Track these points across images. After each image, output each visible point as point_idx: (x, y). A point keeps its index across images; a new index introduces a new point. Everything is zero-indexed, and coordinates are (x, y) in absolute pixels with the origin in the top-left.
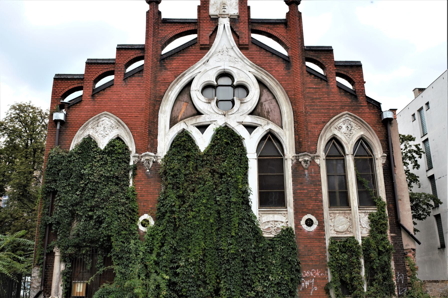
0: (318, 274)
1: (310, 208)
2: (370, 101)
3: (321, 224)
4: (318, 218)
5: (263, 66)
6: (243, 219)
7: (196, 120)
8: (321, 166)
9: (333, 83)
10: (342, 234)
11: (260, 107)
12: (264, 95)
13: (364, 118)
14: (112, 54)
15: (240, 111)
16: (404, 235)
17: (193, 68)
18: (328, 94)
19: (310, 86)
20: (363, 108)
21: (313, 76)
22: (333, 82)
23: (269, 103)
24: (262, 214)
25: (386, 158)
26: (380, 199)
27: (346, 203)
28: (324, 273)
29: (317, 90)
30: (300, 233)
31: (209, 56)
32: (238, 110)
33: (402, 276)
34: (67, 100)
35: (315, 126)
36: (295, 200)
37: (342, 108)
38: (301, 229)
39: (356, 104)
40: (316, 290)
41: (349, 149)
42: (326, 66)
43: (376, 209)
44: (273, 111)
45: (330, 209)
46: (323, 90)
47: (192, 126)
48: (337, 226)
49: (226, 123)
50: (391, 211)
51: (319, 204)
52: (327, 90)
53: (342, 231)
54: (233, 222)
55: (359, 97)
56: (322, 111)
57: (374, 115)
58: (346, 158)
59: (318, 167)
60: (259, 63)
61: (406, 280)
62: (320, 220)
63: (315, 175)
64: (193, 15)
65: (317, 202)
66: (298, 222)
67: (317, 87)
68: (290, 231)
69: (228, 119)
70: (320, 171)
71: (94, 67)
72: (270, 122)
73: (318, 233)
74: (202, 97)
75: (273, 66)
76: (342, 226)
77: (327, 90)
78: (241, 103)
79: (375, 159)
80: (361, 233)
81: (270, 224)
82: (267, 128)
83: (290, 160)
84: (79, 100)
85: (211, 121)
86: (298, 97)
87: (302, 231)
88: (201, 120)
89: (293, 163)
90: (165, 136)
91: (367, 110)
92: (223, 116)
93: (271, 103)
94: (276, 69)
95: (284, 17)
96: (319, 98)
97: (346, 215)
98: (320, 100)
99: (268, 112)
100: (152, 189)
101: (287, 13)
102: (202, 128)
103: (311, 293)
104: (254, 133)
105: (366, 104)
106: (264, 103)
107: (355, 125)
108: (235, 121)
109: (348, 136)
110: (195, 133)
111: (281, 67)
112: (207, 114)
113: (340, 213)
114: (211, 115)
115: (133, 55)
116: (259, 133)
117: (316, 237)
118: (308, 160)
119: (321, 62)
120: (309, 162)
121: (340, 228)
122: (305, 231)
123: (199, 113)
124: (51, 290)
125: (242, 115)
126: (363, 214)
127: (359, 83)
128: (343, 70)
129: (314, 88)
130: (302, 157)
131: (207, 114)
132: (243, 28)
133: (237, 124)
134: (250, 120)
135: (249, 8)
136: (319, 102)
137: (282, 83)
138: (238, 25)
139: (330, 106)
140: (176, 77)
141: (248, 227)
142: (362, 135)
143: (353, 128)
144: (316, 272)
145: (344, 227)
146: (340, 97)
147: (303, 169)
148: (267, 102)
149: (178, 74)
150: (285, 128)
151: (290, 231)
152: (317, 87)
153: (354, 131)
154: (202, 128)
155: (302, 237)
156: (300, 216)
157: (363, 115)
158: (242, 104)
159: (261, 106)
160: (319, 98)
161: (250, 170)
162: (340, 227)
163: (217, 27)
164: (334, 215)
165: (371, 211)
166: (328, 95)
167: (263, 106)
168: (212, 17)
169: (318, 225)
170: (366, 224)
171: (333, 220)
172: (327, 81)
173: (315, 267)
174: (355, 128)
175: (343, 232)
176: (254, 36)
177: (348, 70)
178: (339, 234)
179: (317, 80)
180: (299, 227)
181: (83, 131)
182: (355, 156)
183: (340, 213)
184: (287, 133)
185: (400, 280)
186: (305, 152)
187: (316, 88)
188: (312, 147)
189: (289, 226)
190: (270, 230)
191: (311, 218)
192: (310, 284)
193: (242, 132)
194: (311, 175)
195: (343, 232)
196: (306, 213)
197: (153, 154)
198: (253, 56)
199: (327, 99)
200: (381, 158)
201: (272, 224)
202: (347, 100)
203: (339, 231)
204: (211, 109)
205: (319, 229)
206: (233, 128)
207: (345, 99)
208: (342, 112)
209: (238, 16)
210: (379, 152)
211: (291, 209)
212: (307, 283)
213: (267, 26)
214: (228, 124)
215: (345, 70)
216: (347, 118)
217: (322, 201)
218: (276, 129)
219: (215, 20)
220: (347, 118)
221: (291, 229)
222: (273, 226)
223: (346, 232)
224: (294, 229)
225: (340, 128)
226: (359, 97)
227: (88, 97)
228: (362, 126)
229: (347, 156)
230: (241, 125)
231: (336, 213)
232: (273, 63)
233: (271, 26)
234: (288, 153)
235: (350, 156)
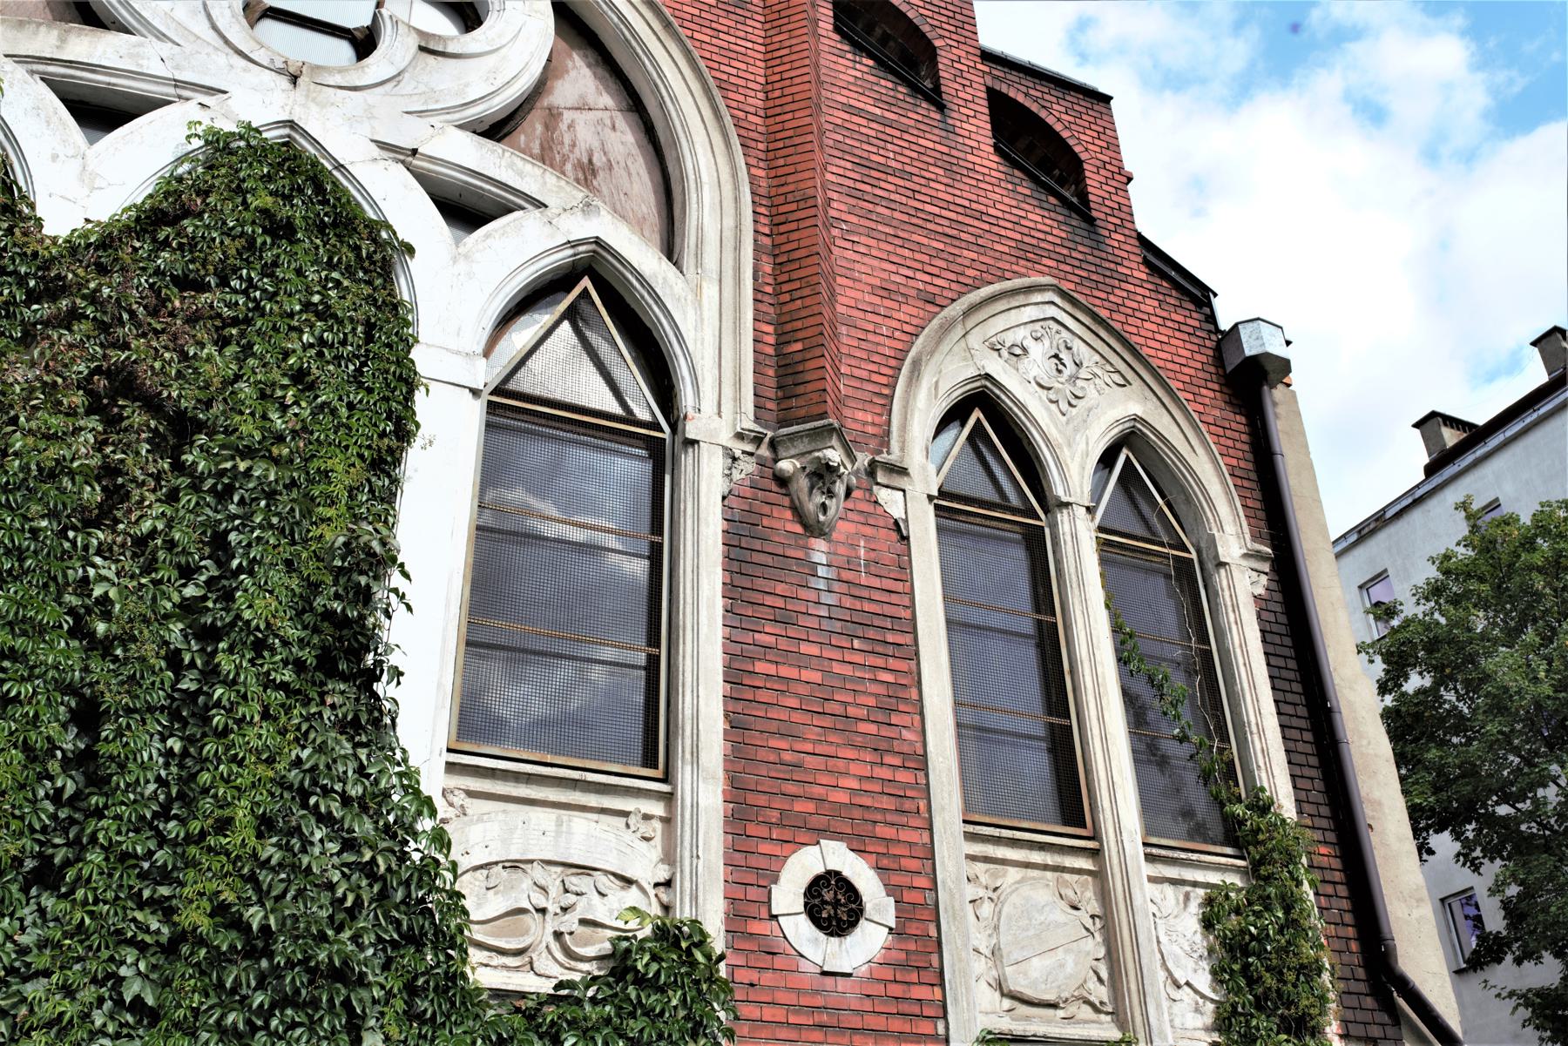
1: (842, 797)
2: (1158, 263)
3: (913, 928)
4: (896, 879)
6: (304, 794)
7: (63, 40)
8: (914, 533)
10: (1049, 1021)
11: (539, 128)
12: (573, 74)
15: (407, 85)
19: (852, 102)
21: (871, 63)
23: (600, 122)
24: (471, 794)
25: (1266, 567)
26: (1263, 807)
30: (767, 978)
35: (877, 300)
36: (736, 725)
37: (1028, 254)
38: (772, 952)
42: (937, 43)
43: (1237, 869)
44: (619, 171)
45: (970, 828)
47: (20, 71)
48: (1017, 956)
50: (1329, 889)
51: (903, 776)
53: (1050, 997)
54: (207, 804)
58: (1054, 526)
59: (900, 532)
62: (909, 896)
63: (876, 582)
65: (888, 759)
66: (753, 893)
68: (688, 950)
69: (314, 108)
70: (904, 568)
76: (1048, 961)
79: (1210, 566)
81: (526, 884)
83: (720, 451)
85: (178, 84)
86: (788, 125)
87: (779, 962)
89: (736, 476)
91: (1150, 305)
92: (284, 82)
93: (614, 128)
97: (1067, 884)
104: (487, 236)
105: (1144, 276)
106: (568, 116)
107: (1097, 358)
108: (366, 131)
109: (1064, 406)
112: (162, 36)
113: (1027, 865)
114: (188, 47)
117: (878, 1023)
119: (909, 14)
121: (1032, 977)
122: (804, 966)
125: (420, 113)
126: (1168, 889)
129: (873, 119)
130: (802, 446)
131: (162, 36)
133: (376, 151)
141: (348, 869)
142: (1136, 419)
143: (1083, 373)
145: (1062, 966)
146: (1014, 203)
147: (799, 529)
150: (699, 263)
151: (689, 952)
153: (1091, 392)
155: (779, 1014)
156: (765, 848)
158: (431, 59)
161: (415, 460)
162: (1038, 967)
164: (995, 876)
165: (1214, 878)
167: (563, 126)
170: (1191, 964)
171: (986, 909)
172: (941, 107)
174: (1095, 375)
175: (1054, 1006)
178: (1027, 1018)
179: (890, 85)
180: (755, 927)
182: (1101, 529)
183: (1027, 865)
184: (710, 291)
186: (823, 415)
188: (860, 415)
189: (683, 912)
190: (526, 932)
191: (846, 873)
194: (846, 575)
195: (1054, 1006)
196: (819, 833)
199: (942, 187)
200: (1245, 563)
201: (544, 889)
203: (1030, 993)
204: (202, 16)
206: (340, 167)
207: (1039, 219)
210: (1230, 528)
214: (306, 134)
216: (1052, 311)
217: (920, 762)
220: (1052, 311)
221: (702, 941)
222: (553, 908)
223: (1072, 1009)
224: (718, 945)
225: (1018, 351)
228: (1130, 375)
229: (1063, 518)
230: (400, 166)
231: (1004, 862)
234: (709, 405)
235: (1081, 512)
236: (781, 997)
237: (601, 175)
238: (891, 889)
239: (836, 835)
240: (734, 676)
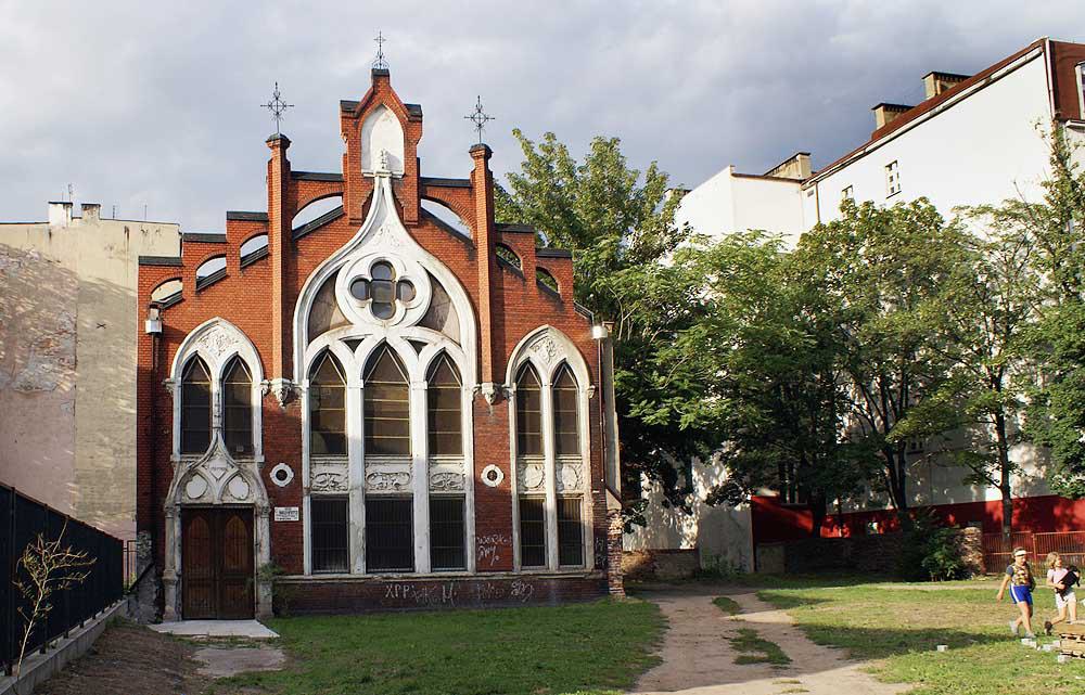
14: (221, 227)
16: (607, 491)
18: (524, 297)
34: (157, 296)
41: (546, 378)
64: (338, 169)
71: (196, 246)
74: (353, 300)
84: (177, 301)
88: (353, 333)
102: (353, 344)
110: (341, 351)
116: (429, 353)
123: (347, 323)
124: (164, 561)
132: (410, 193)
135: (418, 159)
139: (525, 316)
154: (353, 344)
173: (498, 532)
176: (425, 204)
192: (491, 552)
193: (406, 352)
202: (549, 307)
212: (487, 552)
213: (442, 189)
218: (452, 350)
227: (190, 295)
233: (449, 191)
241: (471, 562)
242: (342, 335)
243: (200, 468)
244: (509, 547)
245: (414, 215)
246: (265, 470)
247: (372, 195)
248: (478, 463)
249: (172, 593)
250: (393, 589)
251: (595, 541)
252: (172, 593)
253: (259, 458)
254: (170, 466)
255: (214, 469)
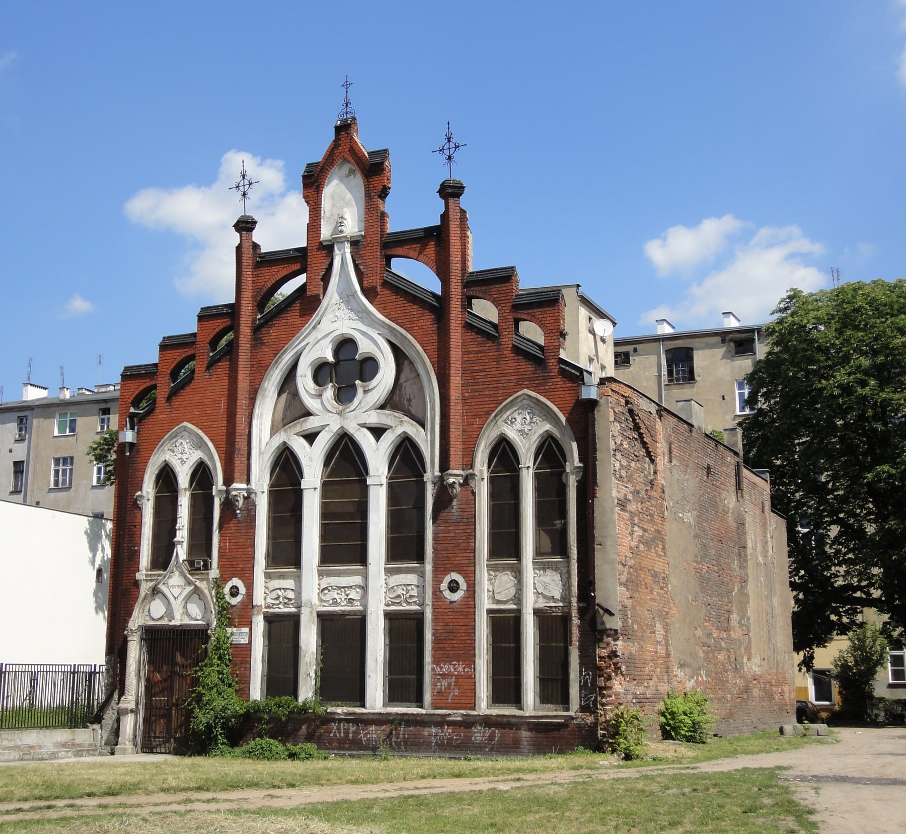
0: (461, 669)
5: (400, 321)
9: (507, 339)
13: (554, 400)
15: (363, 404)
17: (298, 338)
20: (554, 380)
22: (507, 336)
27: (515, 551)
28: (470, 668)
29: (480, 355)
31: (320, 314)
32: (360, 403)
33: (589, 675)
39: (541, 374)
40: (456, 694)
46: (490, 354)
49: (342, 427)
52: (497, 353)
55: (548, 361)
56: (485, 393)
57: (571, 392)
60: (395, 316)
61: (594, 681)
66: (438, 586)
67: (481, 349)
72: (406, 418)
73: (466, 603)
75: (415, 319)
77: (497, 353)
78: (364, 391)
80: (536, 602)
82: (399, 430)
90: (260, 456)
94: (419, 325)
95: (438, 222)
96: (483, 370)
98: (485, 373)
99: (409, 400)
100: (242, 540)
101: (441, 215)
102: (311, 437)
103: (450, 698)
110: (299, 446)
111: (427, 321)
115: (219, 324)
116: (389, 440)
118: (454, 483)
120: (457, 486)
123: (308, 414)
127: (551, 335)
128: (526, 312)
131: (318, 415)
134: (374, 418)
136: (485, 376)
137: (428, 348)
138: (362, 252)
140: (276, 355)
144: (459, 665)
148: (409, 383)
149: (277, 352)
152: (481, 349)
154: (311, 437)
156: (440, 576)
157: (552, 394)
159: (400, 391)
160: (483, 370)
163: (332, 260)
166: (498, 362)
168: (324, 244)
169: (468, 590)
171: (493, 581)
177: (534, 311)
181: (157, 455)
185: (586, 682)
187: (479, 352)
192: (449, 685)
193: (365, 440)
197: (244, 486)
198: (386, 305)
199: (494, 369)
202: (528, 367)
205: (468, 598)
208: (516, 392)
209: (364, 237)
211: (429, 567)
212: (445, 683)
215: (530, 311)
219: (328, 249)
226: (548, 361)
232: (415, 313)
236: (443, 607)
237: (413, 401)
238: (466, 581)
239: (453, 571)
240: (435, 539)
241: (428, 697)
242: (298, 429)
243: (162, 587)
244: (471, 679)
245: (375, 280)
246: (218, 584)
247: (331, 265)
248: (440, 570)
249: (129, 724)
250: (339, 728)
251: (581, 674)
252: (129, 724)
253: (214, 573)
254: (137, 584)
255: (173, 586)
